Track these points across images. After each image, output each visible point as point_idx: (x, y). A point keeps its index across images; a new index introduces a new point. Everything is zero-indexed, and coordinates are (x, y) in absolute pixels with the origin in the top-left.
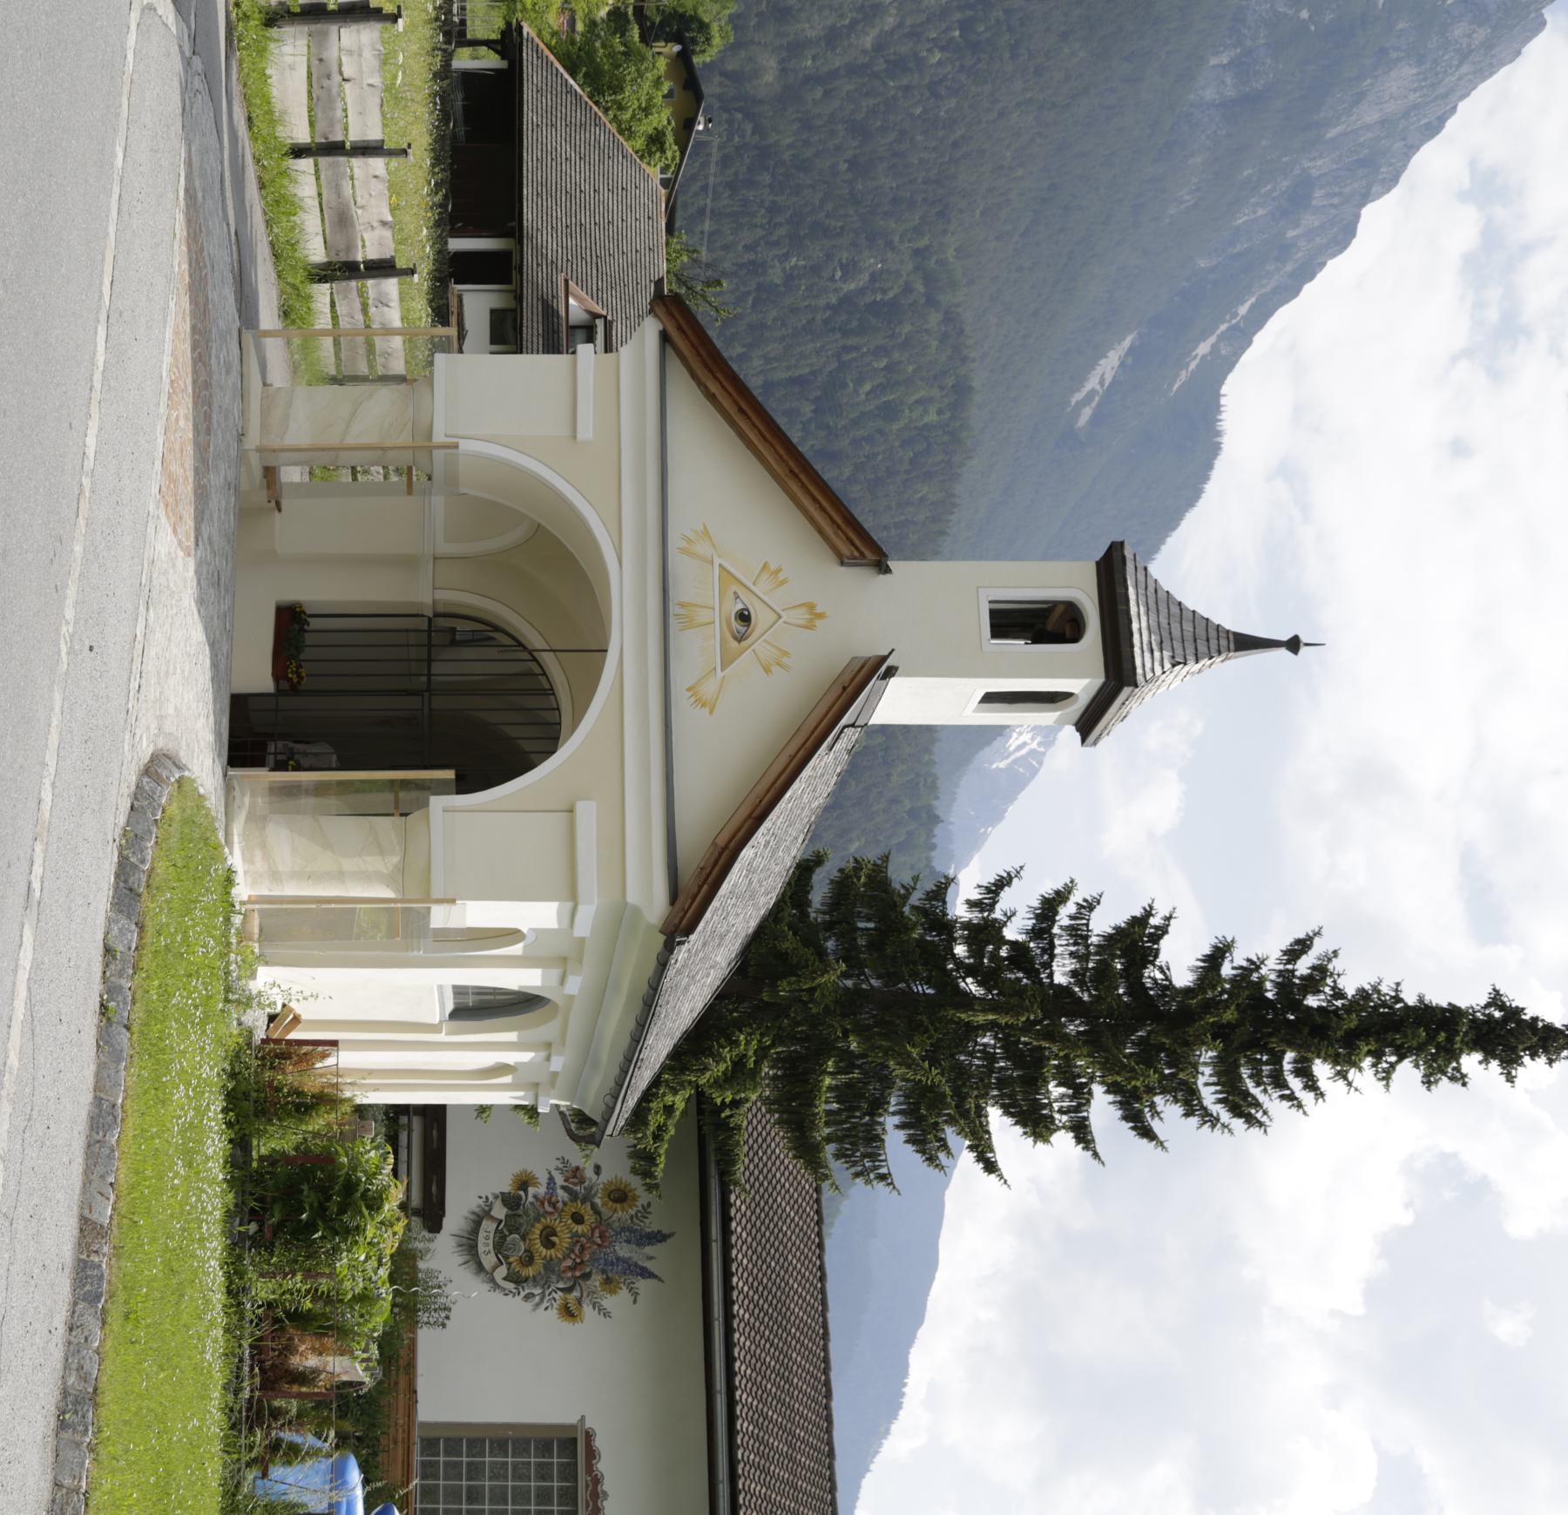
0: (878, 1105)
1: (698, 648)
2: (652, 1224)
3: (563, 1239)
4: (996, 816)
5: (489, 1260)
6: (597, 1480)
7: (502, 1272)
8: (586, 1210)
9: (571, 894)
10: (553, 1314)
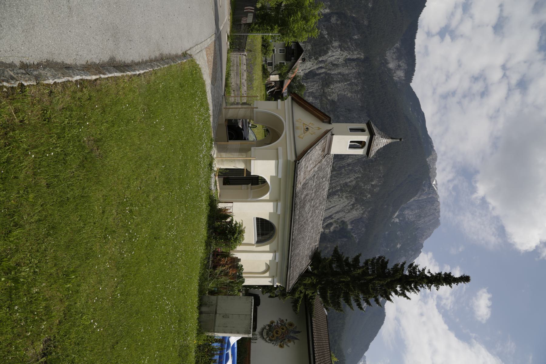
0: (339, 297)
1: (298, 133)
2: (297, 330)
3: (280, 333)
5: (265, 337)
7: (268, 339)
8: (284, 327)
9: (277, 159)
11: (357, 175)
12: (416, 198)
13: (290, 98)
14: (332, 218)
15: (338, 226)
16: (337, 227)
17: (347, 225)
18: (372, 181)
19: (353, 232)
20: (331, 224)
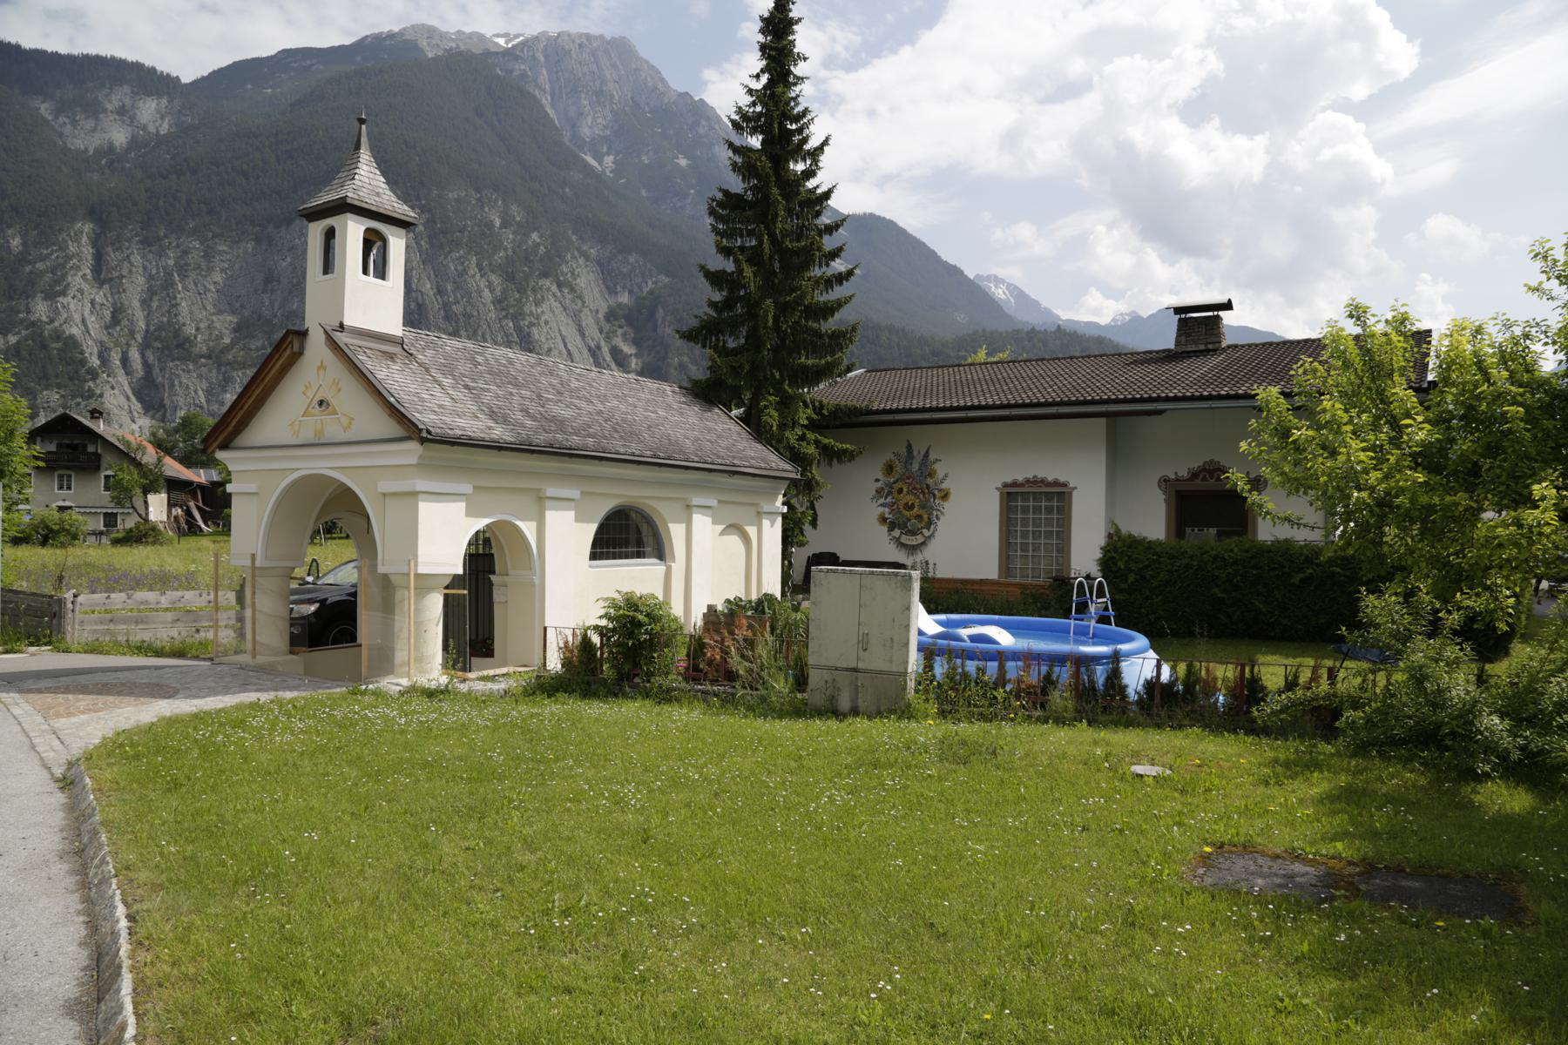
0: (817, 334)
2: (903, 451)
3: (910, 499)
4: (1036, 304)
5: (920, 539)
6: (1028, 481)
8: (897, 487)
9: (414, 495)
10: (946, 504)
11: (473, 270)
12: (546, 100)
13: (221, 455)
14: (599, 348)
15: (620, 332)
16: (624, 335)
17: (620, 305)
18: (490, 225)
19: (640, 287)
20: (615, 352)
